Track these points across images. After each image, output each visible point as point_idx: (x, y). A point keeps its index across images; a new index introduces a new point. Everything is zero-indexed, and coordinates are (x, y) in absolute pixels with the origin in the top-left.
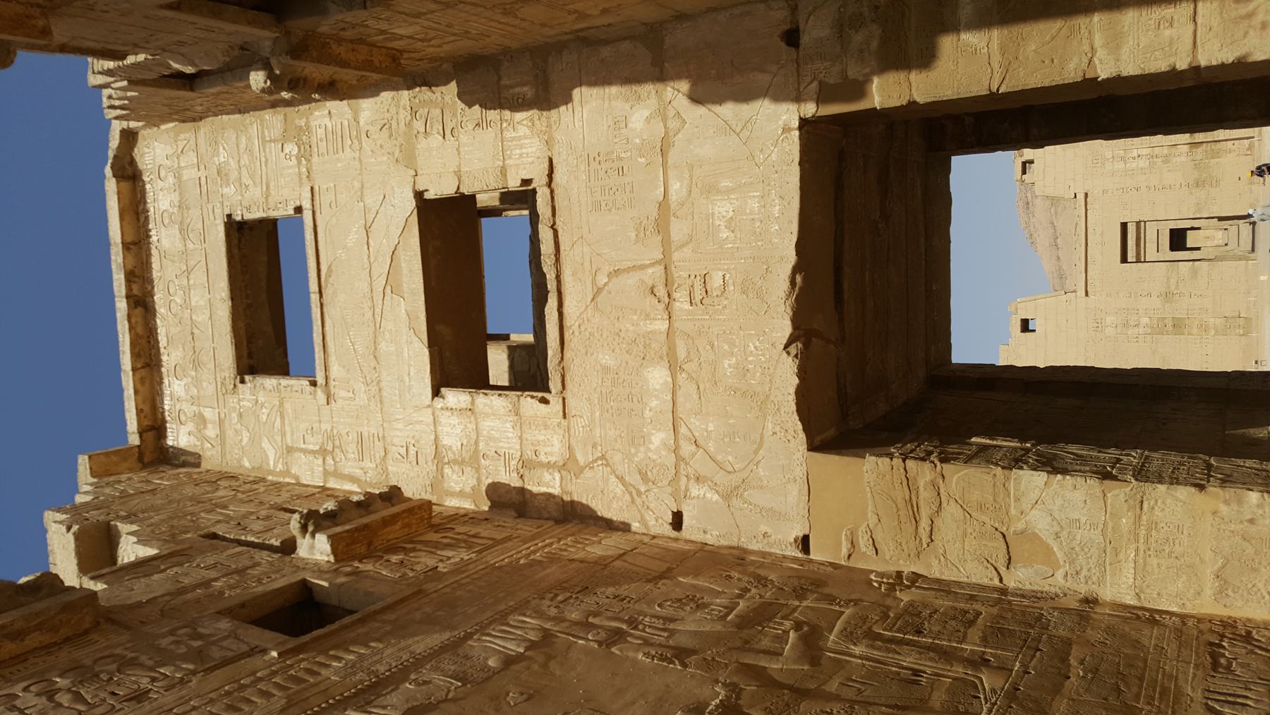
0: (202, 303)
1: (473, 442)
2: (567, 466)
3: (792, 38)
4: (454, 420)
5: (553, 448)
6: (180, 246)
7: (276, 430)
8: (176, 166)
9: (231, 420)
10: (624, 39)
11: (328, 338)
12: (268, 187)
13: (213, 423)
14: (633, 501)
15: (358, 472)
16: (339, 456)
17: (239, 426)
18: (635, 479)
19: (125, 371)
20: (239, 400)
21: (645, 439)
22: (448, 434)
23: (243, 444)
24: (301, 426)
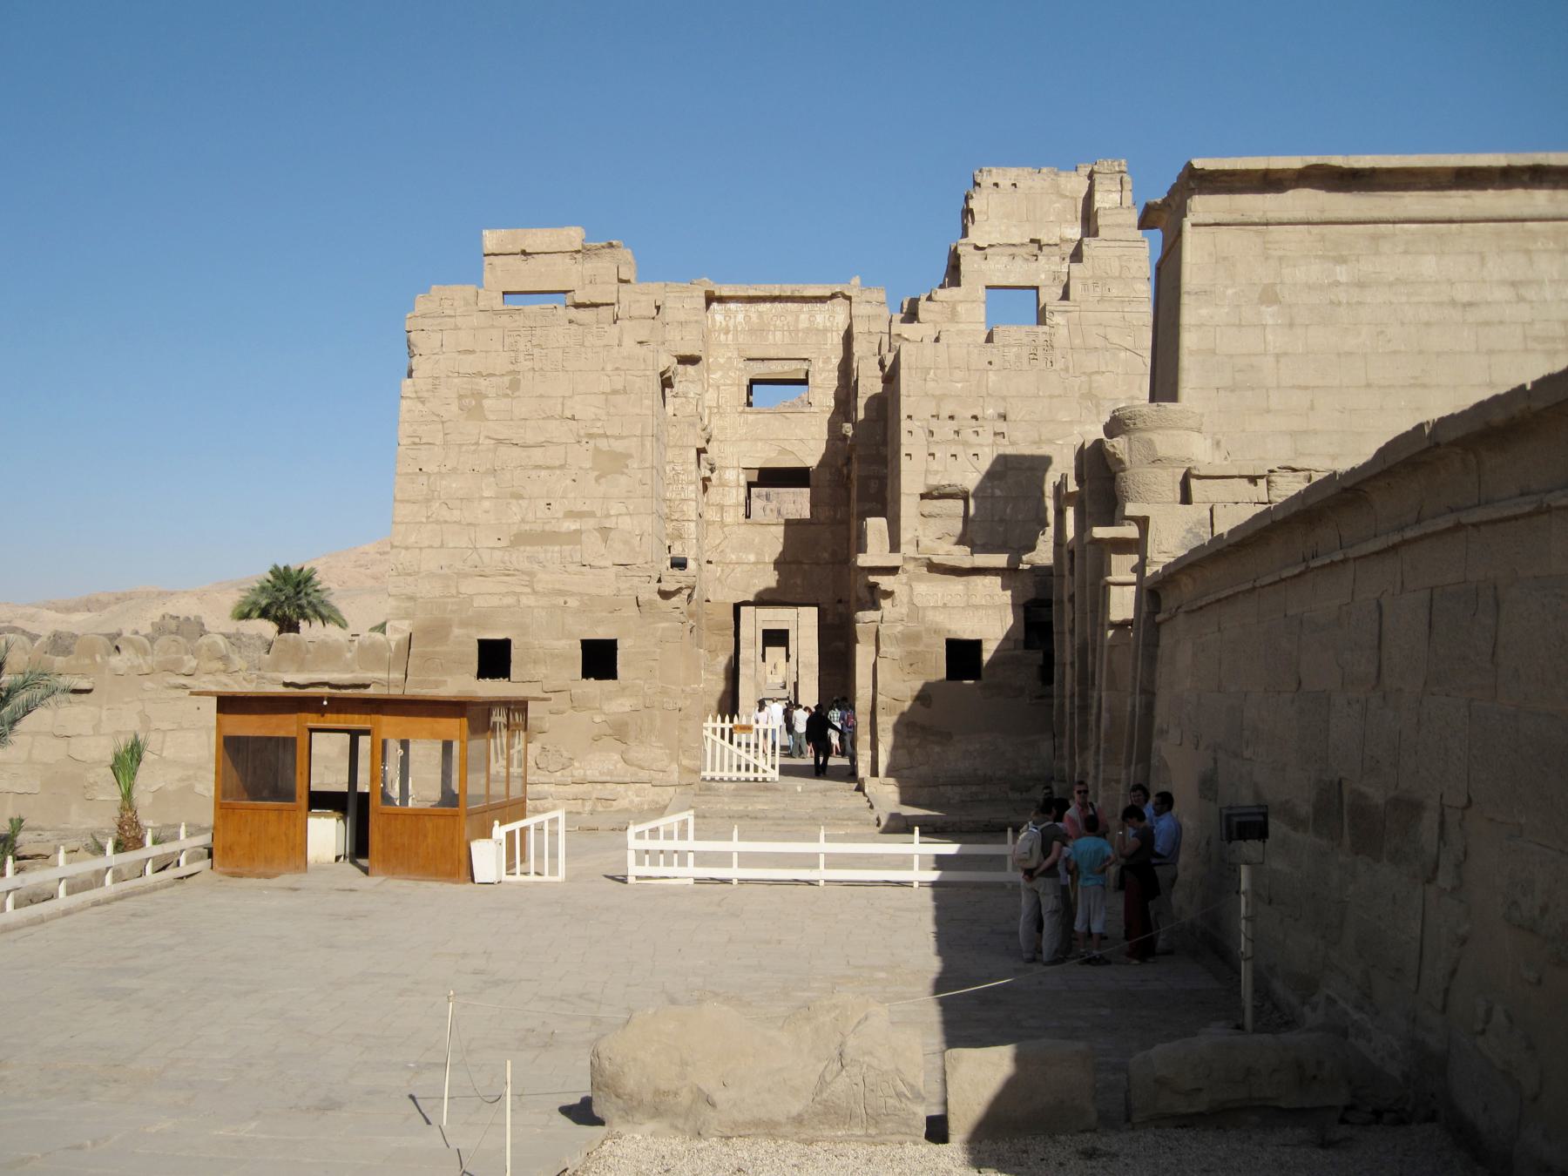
0: (777, 338)
2: (723, 524)
3: (840, 601)
4: (735, 477)
12: (820, 387)
18: (721, 549)
21: (733, 553)
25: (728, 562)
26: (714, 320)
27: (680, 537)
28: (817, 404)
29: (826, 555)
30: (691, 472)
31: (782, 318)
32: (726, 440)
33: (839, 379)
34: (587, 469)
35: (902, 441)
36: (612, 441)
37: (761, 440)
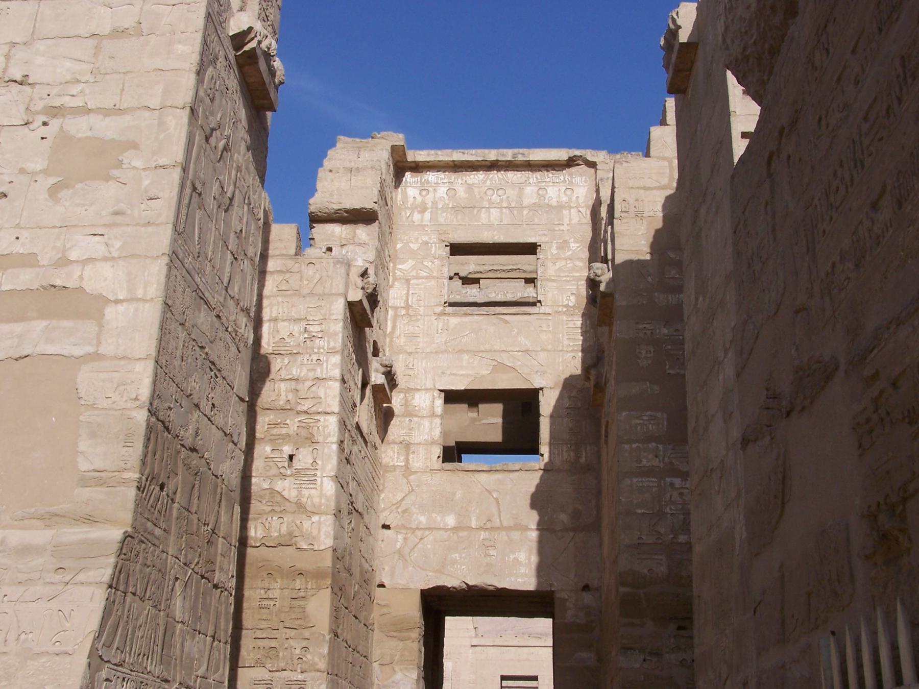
0: (492, 219)
2: (407, 470)
4: (428, 403)
5: (417, 463)
6: (526, 202)
7: (419, 271)
8: (572, 205)
9: (424, 235)
11: (470, 318)
12: (553, 281)
13: (422, 219)
14: (393, 505)
15: (398, 332)
17: (420, 241)
18: (403, 507)
20: (435, 243)
22: (420, 397)
23: (411, 245)
24: (422, 292)
25: (414, 526)
26: (405, 195)
27: (311, 440)
28: (549, 303)
29: (564, 517)
30: (336, 334)
31: (500, 192)
32: (417, 353)
34: (34, 173)
35: (732, 108)
36: (96, 120)
37: (468, 352)
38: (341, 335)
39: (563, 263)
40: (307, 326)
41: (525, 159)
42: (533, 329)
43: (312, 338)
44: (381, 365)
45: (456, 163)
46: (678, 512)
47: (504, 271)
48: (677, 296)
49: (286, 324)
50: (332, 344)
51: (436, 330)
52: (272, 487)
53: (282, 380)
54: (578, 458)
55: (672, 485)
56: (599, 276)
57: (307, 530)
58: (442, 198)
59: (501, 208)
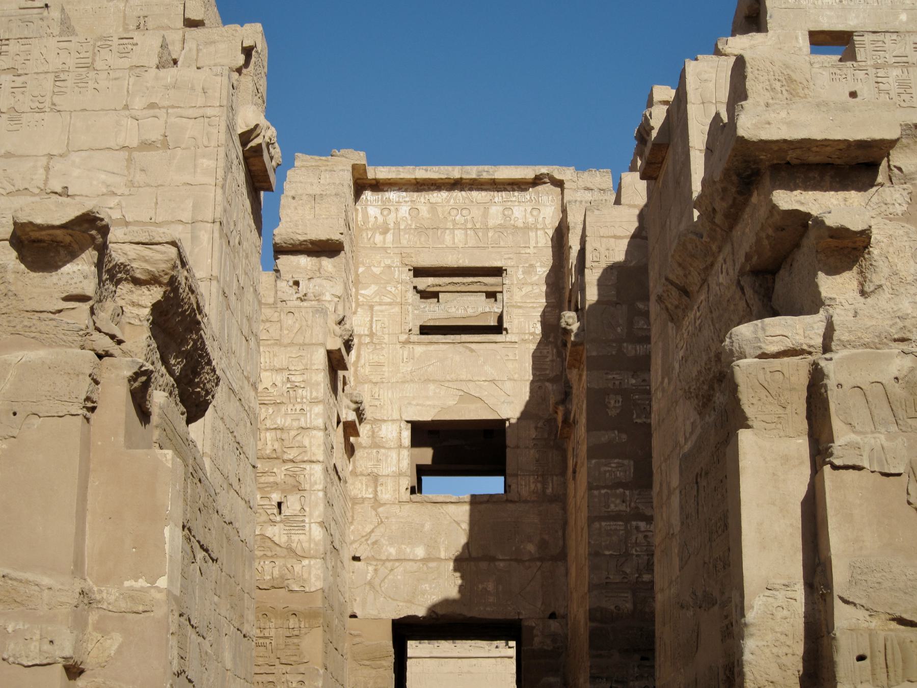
0: (456, 241)
1: (384, 445)
2: (377, 503)
4: (395, 434)
5: (386, 495)
6: (491, 223)
7: (382, 297)
10: (564, 543)
11: (436, 346)
12: (520, 307)
14: (363, 537)
15: (362, 361)
16: (371, 348)
17: (383, 265)
18: (373, 538)
19: (415, 170)
23: (372, 268)
24: (386, 319)
25: (384, 558)
26: (366, 215)
27: (298, 488)
28: (515, 331)
29: (531, 548)
30: (318, 384)
31: (464, 212)
33: (548, 295)
37: (434, 381)
38: (322, 385)
39: (529, 288)
40: (290, 377)
41: (490, 177)
42: (499, 357)
43: (295, 388)
44: (351, 401)
45: (418, 181)
46: (643, 553)
47: (464, 284)
48: (645, 346)
49: (268, 374)
50: (314, 394)
51: (401, 358)
52: (263, 533)
53: (267, 429)
54: (544, 489)
55: (637, 528)
56: (570, 325)
57: (298, 573)
58: (404, 218)
59: (466, 229)
